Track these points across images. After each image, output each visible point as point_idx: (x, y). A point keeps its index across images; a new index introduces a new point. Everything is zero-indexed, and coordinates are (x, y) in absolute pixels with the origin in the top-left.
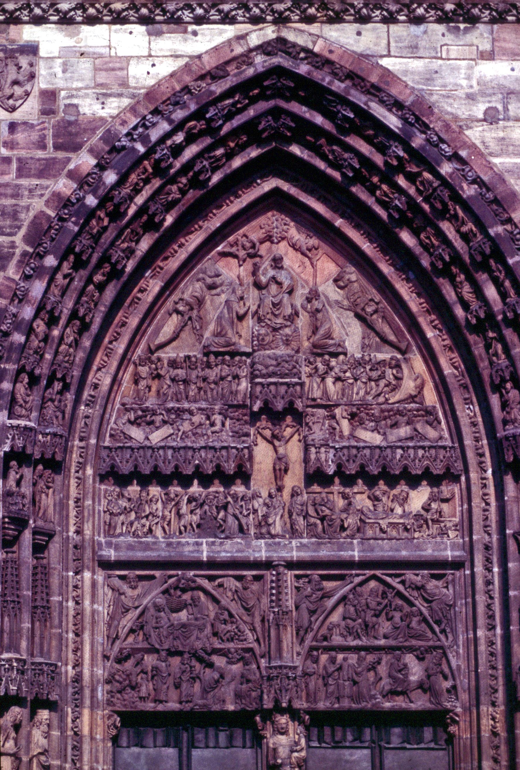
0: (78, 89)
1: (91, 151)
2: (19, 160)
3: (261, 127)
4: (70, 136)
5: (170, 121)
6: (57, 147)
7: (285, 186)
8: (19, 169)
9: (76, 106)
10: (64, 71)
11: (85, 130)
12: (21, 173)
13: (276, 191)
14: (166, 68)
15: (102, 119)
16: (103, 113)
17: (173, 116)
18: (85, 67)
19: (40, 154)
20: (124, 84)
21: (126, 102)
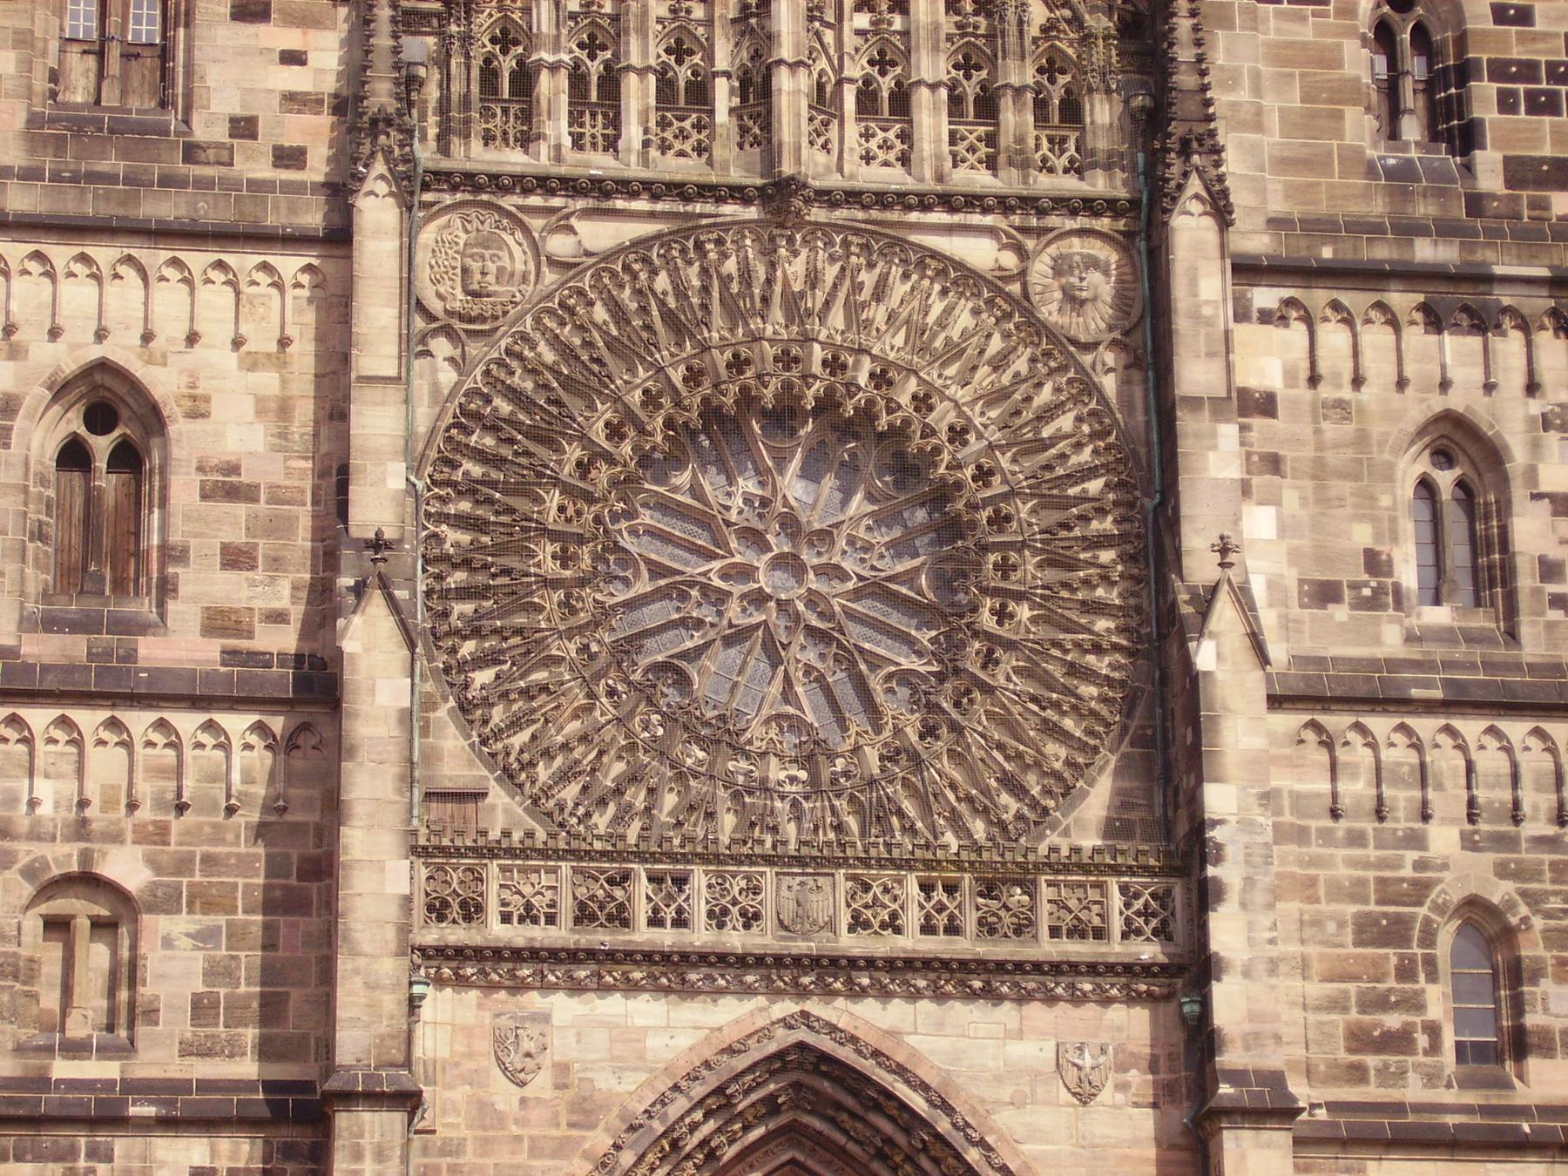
0: (593, 1062)
1: (607, 1130)
2: (532, 1139)
3: (780, 1100)
4: (584, 1112)
5: (690, 1099)
6: (571, 1125)
7: (801, 1158)
8: (531, 1149)
9: (592, 1080)
10: (578, 1042)
11: (601, 1107)
12: (534, 1151)
13: (792, 1161)
14: (684, 1041)
15: (618, 1095)
16: (620, 1089)
17: (692, 1093)
18: (600, 1038)
19: (554, 1132)
20: (641, 1057)
21: (644, 1076)
